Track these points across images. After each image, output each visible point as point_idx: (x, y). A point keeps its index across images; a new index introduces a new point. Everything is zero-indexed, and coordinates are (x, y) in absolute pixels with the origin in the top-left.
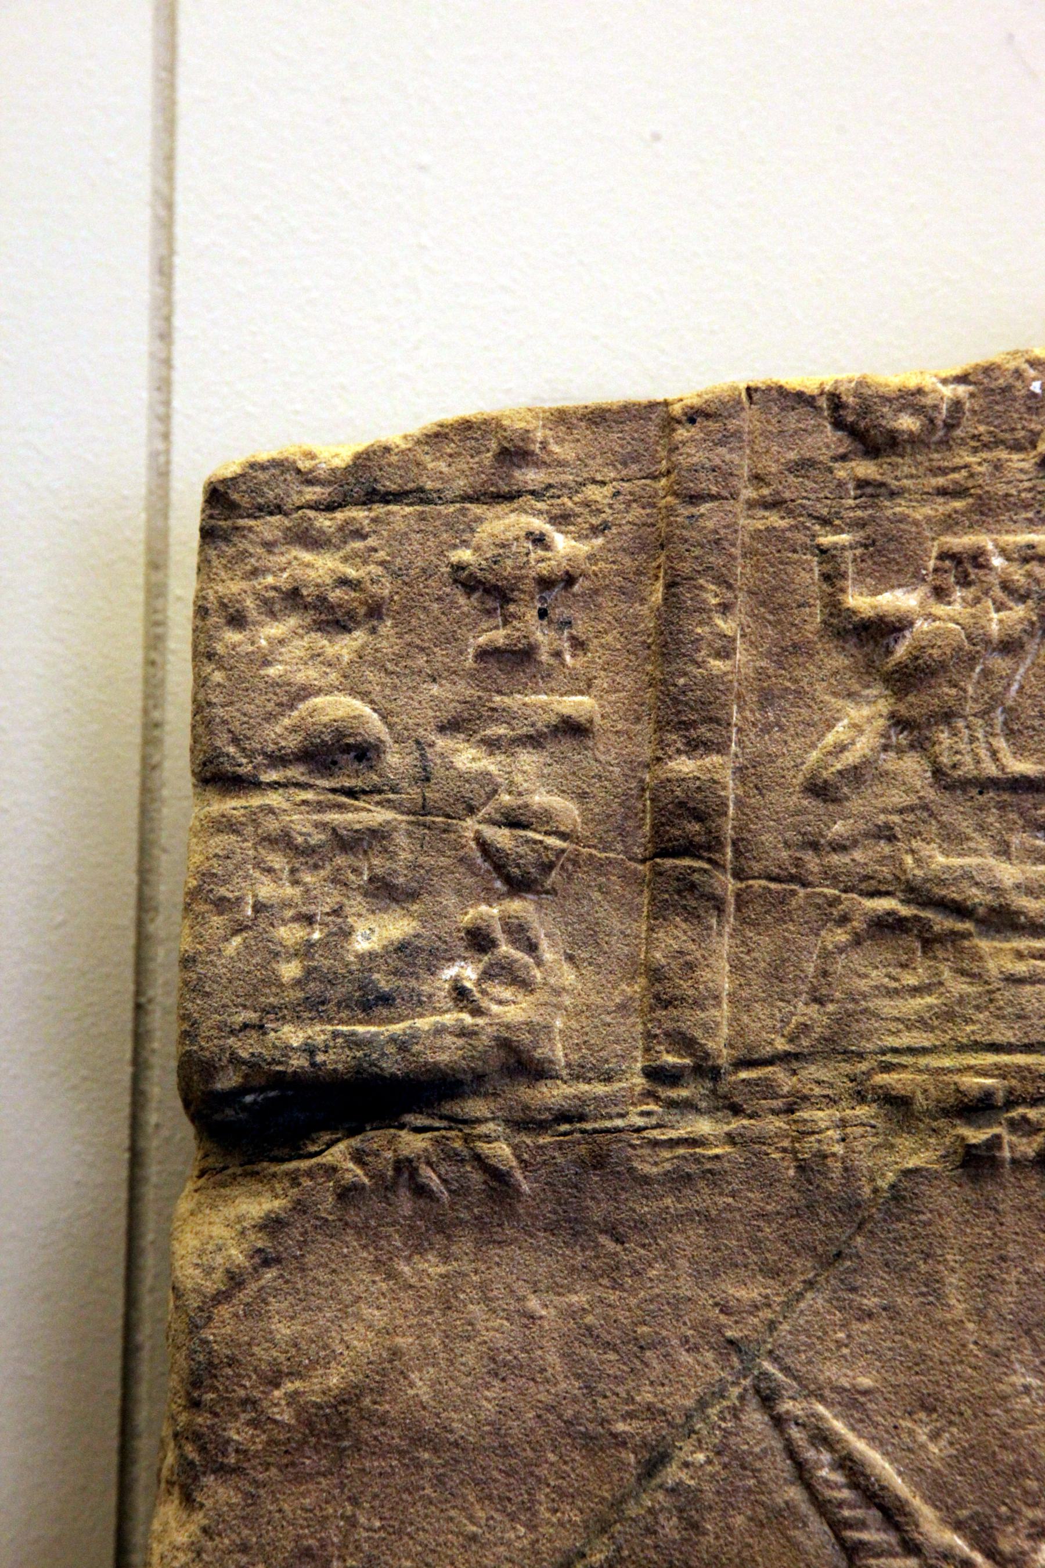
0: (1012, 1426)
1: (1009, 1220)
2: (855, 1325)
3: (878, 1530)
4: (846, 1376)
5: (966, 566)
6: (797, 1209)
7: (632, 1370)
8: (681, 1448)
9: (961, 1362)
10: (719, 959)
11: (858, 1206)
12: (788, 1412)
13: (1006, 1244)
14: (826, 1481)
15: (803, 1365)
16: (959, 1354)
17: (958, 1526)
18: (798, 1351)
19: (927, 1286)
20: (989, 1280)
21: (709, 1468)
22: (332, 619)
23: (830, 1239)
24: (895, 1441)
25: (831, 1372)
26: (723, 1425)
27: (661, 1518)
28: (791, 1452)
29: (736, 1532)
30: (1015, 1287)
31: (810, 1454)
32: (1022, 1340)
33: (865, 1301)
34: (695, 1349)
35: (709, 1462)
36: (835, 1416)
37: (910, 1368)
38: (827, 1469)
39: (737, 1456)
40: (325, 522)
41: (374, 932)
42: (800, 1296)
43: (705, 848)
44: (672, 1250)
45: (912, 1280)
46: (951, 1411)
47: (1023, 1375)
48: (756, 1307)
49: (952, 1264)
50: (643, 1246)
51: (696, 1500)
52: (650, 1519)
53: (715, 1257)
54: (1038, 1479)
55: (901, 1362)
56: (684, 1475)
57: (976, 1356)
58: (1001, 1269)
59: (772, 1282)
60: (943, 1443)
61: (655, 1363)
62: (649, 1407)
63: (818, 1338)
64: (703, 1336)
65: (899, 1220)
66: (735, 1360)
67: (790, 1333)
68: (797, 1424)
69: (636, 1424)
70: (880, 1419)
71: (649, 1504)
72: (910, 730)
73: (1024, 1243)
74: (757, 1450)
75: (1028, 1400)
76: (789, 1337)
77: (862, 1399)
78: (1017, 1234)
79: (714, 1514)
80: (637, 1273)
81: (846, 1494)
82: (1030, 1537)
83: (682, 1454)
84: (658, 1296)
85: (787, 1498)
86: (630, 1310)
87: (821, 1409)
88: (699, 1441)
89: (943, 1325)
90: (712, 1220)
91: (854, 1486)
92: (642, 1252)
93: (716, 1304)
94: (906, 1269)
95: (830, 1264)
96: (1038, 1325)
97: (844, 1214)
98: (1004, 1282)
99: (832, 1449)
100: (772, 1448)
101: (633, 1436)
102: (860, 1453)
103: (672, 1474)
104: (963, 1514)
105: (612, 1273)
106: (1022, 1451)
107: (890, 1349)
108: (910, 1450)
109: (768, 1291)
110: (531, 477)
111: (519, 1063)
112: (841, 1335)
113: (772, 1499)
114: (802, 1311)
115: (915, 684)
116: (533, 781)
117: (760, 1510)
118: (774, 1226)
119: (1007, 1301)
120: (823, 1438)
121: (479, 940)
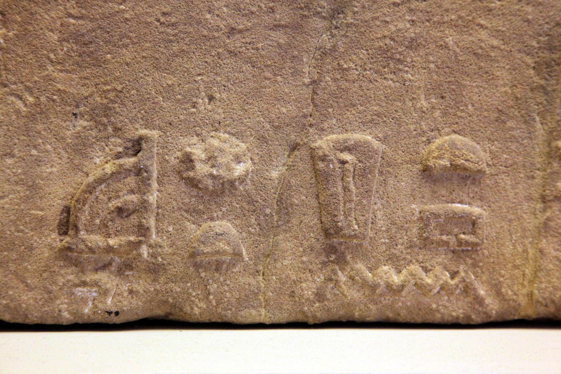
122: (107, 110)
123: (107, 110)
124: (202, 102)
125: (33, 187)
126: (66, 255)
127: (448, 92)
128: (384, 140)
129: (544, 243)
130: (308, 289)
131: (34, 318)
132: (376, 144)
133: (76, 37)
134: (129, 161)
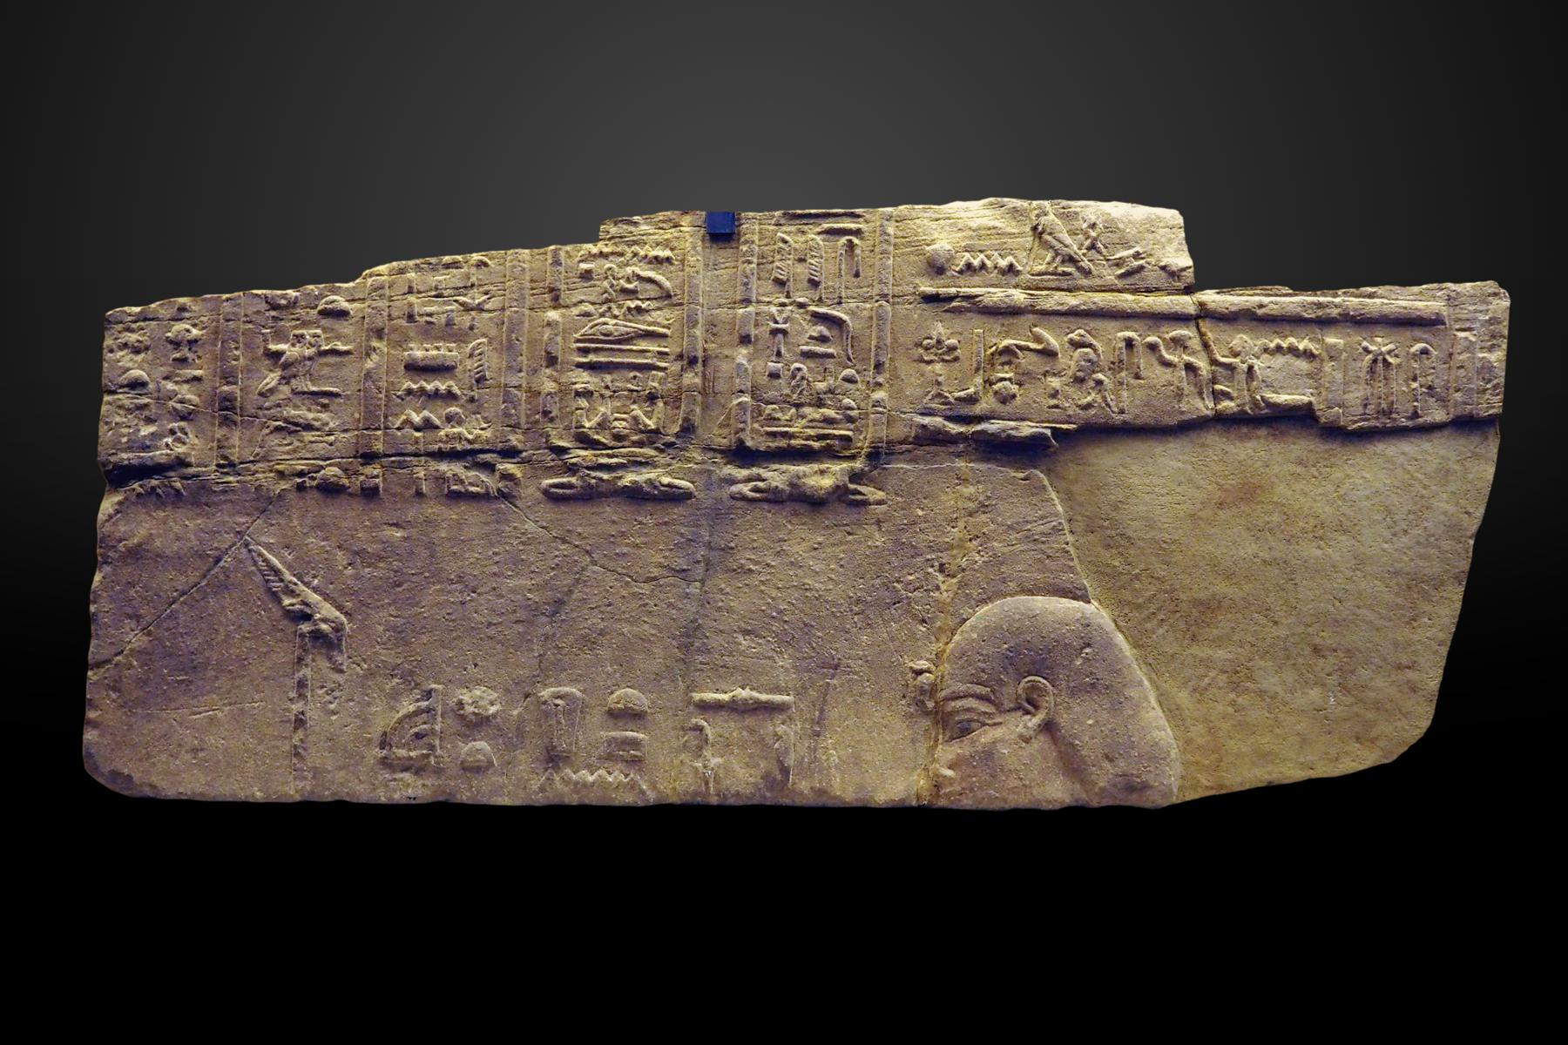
5: (299, 338)
10: (236, 438)
22: (137, 351)
25: (263, 539)
40: (134, 326)
41: (146, 430)
43: (232, 409)
72: (285, 380)
103: (222, 564)
105: (207, 515)
110: (187, 315)
111: (181, 462)
115: (289, 369)
116: (186, 392)
120: (260, 555)
121: (172, 432)
122: (411, 673)
124: (470, 667)
126: (385, 763)
127: (624, 662)
128: (583, 692)
129: (683, 756)
130: (535, 785)
132: (579, 694)
133: (394, 628)
134: (424, 704)
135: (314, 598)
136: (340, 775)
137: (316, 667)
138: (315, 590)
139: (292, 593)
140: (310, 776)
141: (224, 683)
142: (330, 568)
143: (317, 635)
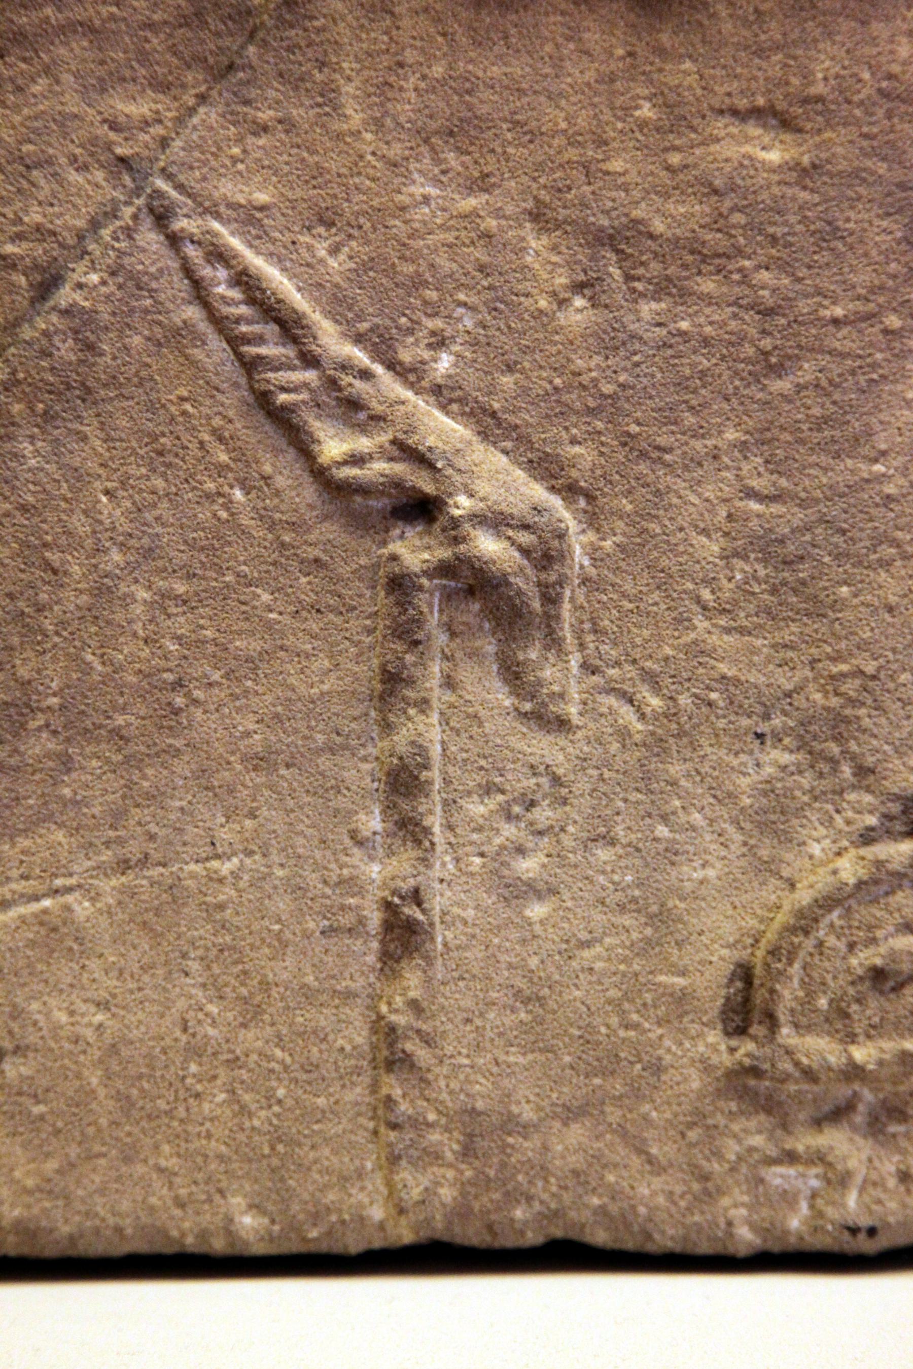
0: (411, 237)
1: (406, 23)
2: (250, 140)
3: (276, 344)
4: (241, 191)
6: (184, 17)
7: (19, 190)
8: (73, 270)
9: (359, 174)
11: (249, 12)
12: (182, 230)
13: (403, 49)
14: (223, 297)
15: (198, 181)
16: (356, 165)
17: (359, 339)
18: (191, 168)
19: (322, 95)
20: (386, 88)
21: (103, 289)
23: (219, 48)
24: (294, 257)
25: (227, 189)
26: (117, 245)
27: (56, 340)
28: (188, 271)
29: (133, 352)
30: (413, 95)
31: (206, 272)
32: (422, 149)
33: (260, 114)
34: (85, 168)
35: (104, 283)
36: (232, 234)
37: (307, 182)
38: (223, 286)
39: (131, 276)
42: (192, 111)
44: (54, 62)
45: (307, 90)
46: (349, 224)
47: (423, 185)
48: (146, 122)
49: (348, 72)
50: (24, 60)
51: (91, 321)
52: (44, 342)
53: (101, 72)
54: (437, 289)
55: (299, 177)
56: (78, 297)
57: (374, 167)
58: (398, 76)
59: (161, 96)
60: (342, 257)
61: (42, 182)
62: (38, 228)
63: (213, 154)
64: (92, 154)
65: (292, 27)
66: (127, 179)
67: (183, 149)
68: (192, 242)
69: (25, 245)
70: (277, 235)
71: (43, 326)
73: (422, 49)
74: (153, 270)
75: (427, 210)
76: (182, 154)
77: (258, 215)
78: (414, 38)
79: (111, 335)
80: (20, 89)
81: (243, 310)
82: (430, 346)
83: (75, 276)
84: (43, 112)
85: (184, 317)
86: (14, 127)
87: (216, 226)
88: (93, 262)
89: (339, 136)
90: (97, 31)
91: (251, 301)
92: (24, 66)
93: (105, 121)
94: (302, 79)
95: (223, 77)
96: (437, 132)
97: (234, 21)
98: (401, 89)
99: (227, 265)
100: (168, 268)
101: (23, 258)
102: (257, 268)
103: (65, 296)
104: (364, 326)
106: (421, 261)
107: (287, 163)
108: (308, 265)
109: (159, 106)
112: (236, 151)
113: (169, 319)
114: (195, 128)
117: (157, 330)
118: (162, 36)
119: (404, 109)
120: (219, 255)
123: (840, 725)
125: (661, 918)
126: (747, 1087)
131: (667, 1238)
133: (767, 546)
135: (441, 429)
136: (570, 1142)
137: (461, 705)
138: (443, 394)
139: (351, 410)
140: (450, 1147)
141: (94, 780)
142: (501, 303)
143: (472, 583)
